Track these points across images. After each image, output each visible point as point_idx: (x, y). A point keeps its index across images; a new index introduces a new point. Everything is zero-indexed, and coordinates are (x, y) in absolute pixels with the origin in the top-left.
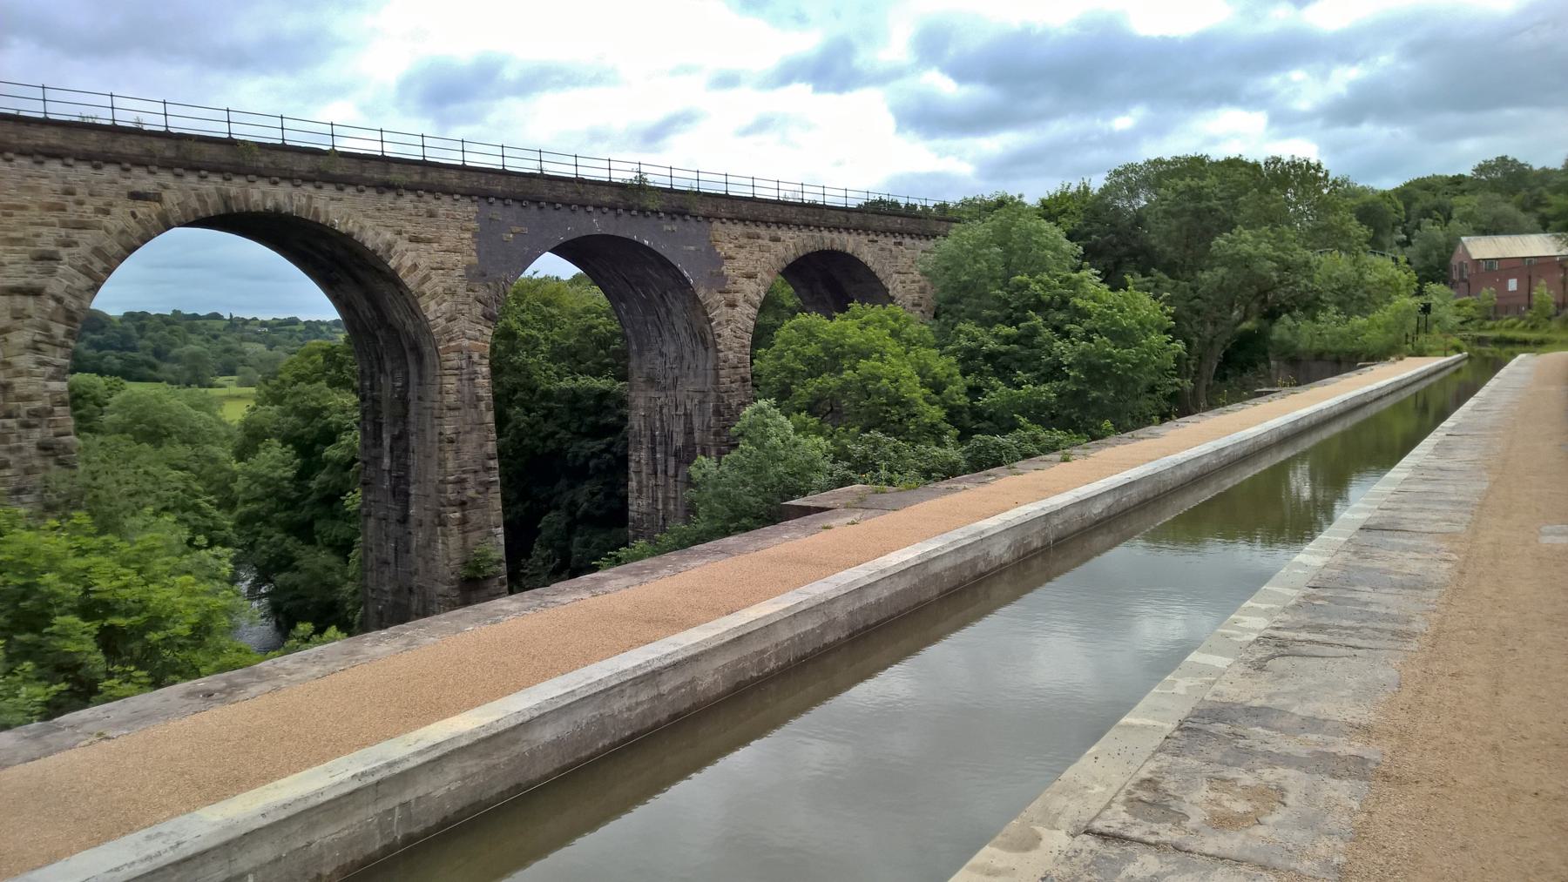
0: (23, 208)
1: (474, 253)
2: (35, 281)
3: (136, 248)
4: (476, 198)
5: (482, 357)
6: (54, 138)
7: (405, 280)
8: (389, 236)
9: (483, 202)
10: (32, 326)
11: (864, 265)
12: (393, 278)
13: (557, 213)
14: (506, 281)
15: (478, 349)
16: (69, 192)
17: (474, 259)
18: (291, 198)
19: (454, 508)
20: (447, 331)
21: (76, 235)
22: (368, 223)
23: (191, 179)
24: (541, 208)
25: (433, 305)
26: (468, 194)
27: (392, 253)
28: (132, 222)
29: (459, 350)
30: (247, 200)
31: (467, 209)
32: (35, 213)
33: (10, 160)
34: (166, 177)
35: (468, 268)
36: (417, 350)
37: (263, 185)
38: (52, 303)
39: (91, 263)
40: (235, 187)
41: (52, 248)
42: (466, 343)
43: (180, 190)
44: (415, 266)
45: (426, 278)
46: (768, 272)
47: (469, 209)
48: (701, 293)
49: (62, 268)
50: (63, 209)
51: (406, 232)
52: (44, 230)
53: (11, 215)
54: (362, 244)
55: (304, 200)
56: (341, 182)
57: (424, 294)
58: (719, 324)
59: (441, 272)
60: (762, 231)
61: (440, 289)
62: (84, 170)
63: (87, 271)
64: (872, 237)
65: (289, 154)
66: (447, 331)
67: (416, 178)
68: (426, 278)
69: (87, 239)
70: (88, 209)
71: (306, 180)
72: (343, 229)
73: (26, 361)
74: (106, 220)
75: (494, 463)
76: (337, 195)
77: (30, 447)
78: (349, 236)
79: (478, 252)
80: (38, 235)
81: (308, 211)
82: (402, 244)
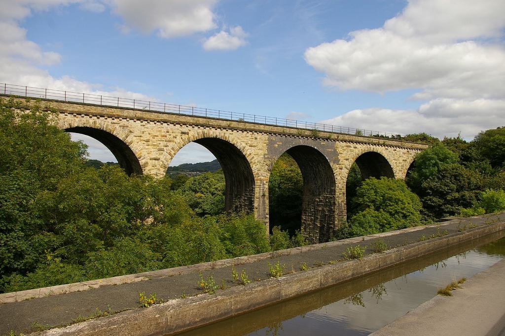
0: (157, 136)
2: (158, 156)
5: (266, 182)
8: (244, 144)
10: (156, 168)
11: (383, 158)
12: (243, 158)
15: (265, 180)
16: (168, 132)
17: (266, 152)
18: (220, 133)
20: (258, 174)
21: (168, 144)
22: (239, 141)
23: (196, 128)
24: (286, 137)
28: (182, 141)
29: (261, 180)
31: (266, 136)
33: (155, 123)
34: (190, 128)
36: (246, 179)
37: (213, 130)
38: (161, 163)
40: (207, 130)
42: (262, 178)
44: (250, 154)
45: (253, 157)
46: (353, 158)
48: (331, 164)
49: (165, 153)
50: (166, 137)
56: (233, 129)
58: (337, 175)
60: (351, 144)
63: (170, 154)
64: (386, 147)
66: (258, 174)
67: (252, 128)
68: (253, 157)
69: (171, 145)
70: (172, 136)
74: (175, 140)
75: (268, 216)
76: (231, 132)
78: (233, 145)
82: (247, 147)
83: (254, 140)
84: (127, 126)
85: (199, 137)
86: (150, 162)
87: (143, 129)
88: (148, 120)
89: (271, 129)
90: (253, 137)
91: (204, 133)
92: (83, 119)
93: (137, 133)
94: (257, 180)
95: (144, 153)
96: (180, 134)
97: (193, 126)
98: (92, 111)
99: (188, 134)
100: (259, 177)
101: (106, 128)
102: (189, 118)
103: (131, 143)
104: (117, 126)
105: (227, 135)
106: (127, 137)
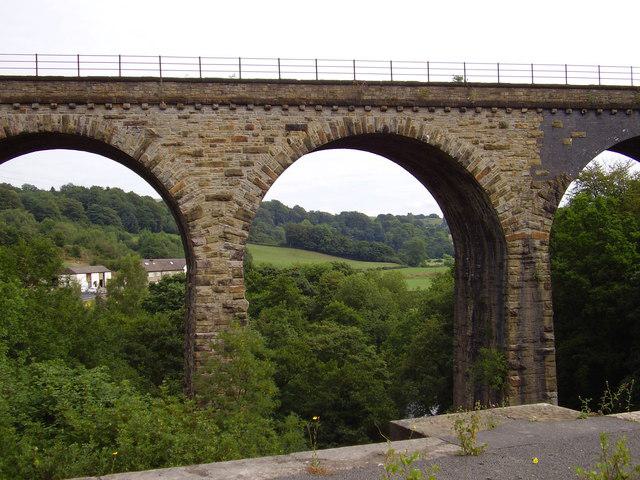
0: (222, 141)
1: (538, 157)
3: (289, 165)
4: (540, 110)
5: (542, 243)
6: (241, 92)
7: (480, 181)
8: (468, 146)
9: (546, 113)
12: (470, 179)
13: (613, 118)
14: (565, 178)
15: (539, 237)
16: (249, 128)
17: (538, 162)
18: (395, 121)
19: (513, 372)
20: (513, 222)
21: (252, 158)
22: (452, 136)
23: (327, 113)
25: (501, 200)
26: (533, 107)
27: (470, 160)
30: (364, 124)
31: (533, 120)
32: (228, 145)
34: (310, 113)
35: (533, 168)
36: (490, 237)
37: (375, 113)
38: (236, 206)
39: (261, 177)
40: (356, 116)
41: (238, 168)
42: (529, 232)
43: (322, 123)
44: (488, 169)
45: (497, 178)
47: (536, 119)
49: (244, 181)
50: (245, 140)
51: (482, 142)
52: (234, 156)
53: (215, 146)
54: (447, 153)
55: (404, 122)
56: (431, 106)
57: (494, 192)
59: (509, 173)
61: (508, 188)
62: (259, 112)
63: (257, 183)
65: (396, 88)
66: (513, 222)
67: (492, 98)
68: (497, 178)
69: (259, 160)
70: (261, 138)
71: (408, 105)
72: (433, 142)
73: (218, 247)
74: (271, 147)
75: (550, 336)
76: (428, 116)
77: (217, 306)
78: (436, 148)
79: (541, 156)
80: (230, 159)
81: (407, 130)
82: (478, 152)
83: (498, 131)
84: (144, 123)
85: (335, 135)
86: (207, 206)
87: (184, 126)
88: (198, 104)
89: (551, 96)
90: (496, 124)
91: (349, 124)
92: (33, 114)
93: (170, 137)
94: (514, 238)
95: (191, 184)
96: (282, 132)
97: (319, 107)
98: (56, 94)
99: (304, 128)
100: (517, 229)
101: (93, 130)
102: (307, 89)
103: (155, 162)
104: (119, 124)
105: (416, 125)
106: (144, 149)
